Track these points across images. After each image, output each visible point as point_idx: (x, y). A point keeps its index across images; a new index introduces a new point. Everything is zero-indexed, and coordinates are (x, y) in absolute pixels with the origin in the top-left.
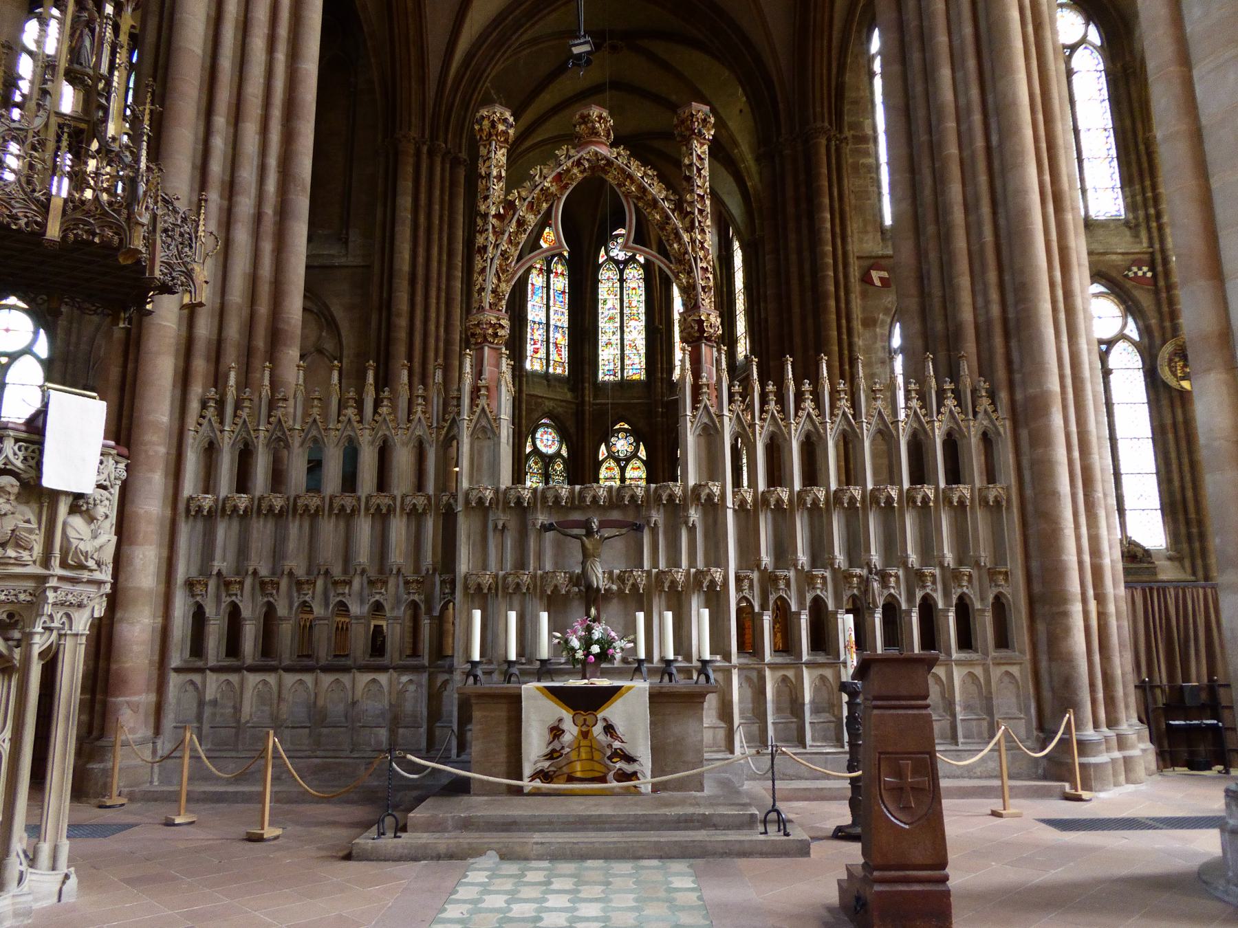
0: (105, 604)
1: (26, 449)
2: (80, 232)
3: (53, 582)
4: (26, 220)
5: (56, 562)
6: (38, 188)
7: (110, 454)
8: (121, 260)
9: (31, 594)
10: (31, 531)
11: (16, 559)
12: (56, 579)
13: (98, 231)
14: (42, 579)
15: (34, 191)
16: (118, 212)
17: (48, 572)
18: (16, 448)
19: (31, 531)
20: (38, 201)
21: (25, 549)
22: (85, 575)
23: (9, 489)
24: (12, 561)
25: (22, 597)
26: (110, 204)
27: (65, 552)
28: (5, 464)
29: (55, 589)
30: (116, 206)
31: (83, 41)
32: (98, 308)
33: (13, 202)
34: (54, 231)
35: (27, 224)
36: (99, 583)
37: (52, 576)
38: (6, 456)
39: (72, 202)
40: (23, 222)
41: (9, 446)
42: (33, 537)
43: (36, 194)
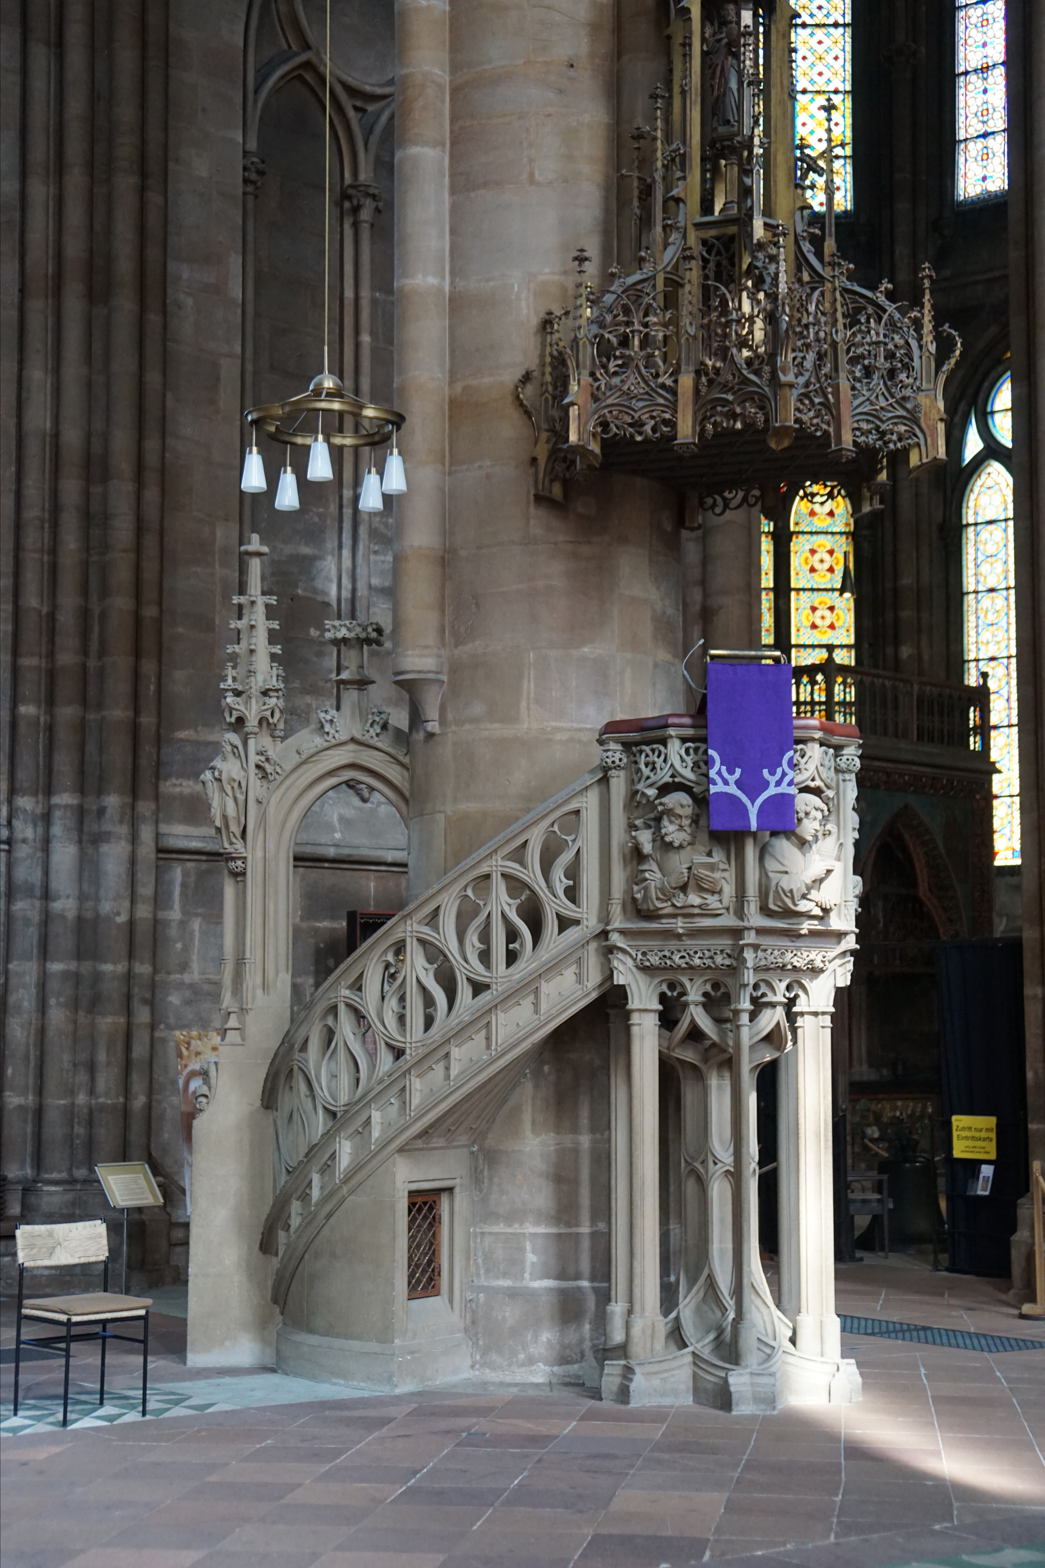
0: (850, 966)
1: (696, 750)
2: (719, 419)
3: (750, 938)
4: (653, 422)
5: (752, 908)
6: (661, 372)
7: (813, 740)
8: (773, 445)
9: (729, 956)
10: (712, 867)
11: (700, 907)
12: (753, 933)
13: (738, 410)
14: (737, 933)
15: (657, 376)
16: (757, 373)
17: (741, 924)
18: (683, 752)
19: (712, 867)
20: (663, 386)
21: (713, 893)
22: (806, 926)
23: (679, 811)
24: (697, 911)
25: (719, 960)
26: (749, 362)
27: (764, 893)
28: (673, 776)
29: (756, 947)
30: (756, 366)
31: (727, 82)
32: (833, 487)
33: (634, 401)
34: (686, 429)
35: (654, 430)
36: (840, 935)
37: (749, 929)
38: (672, 765)
39: (707, 374)
40: (648, 429)
41: (675, 749)
42: (717, 875)
43: (660, 380)
